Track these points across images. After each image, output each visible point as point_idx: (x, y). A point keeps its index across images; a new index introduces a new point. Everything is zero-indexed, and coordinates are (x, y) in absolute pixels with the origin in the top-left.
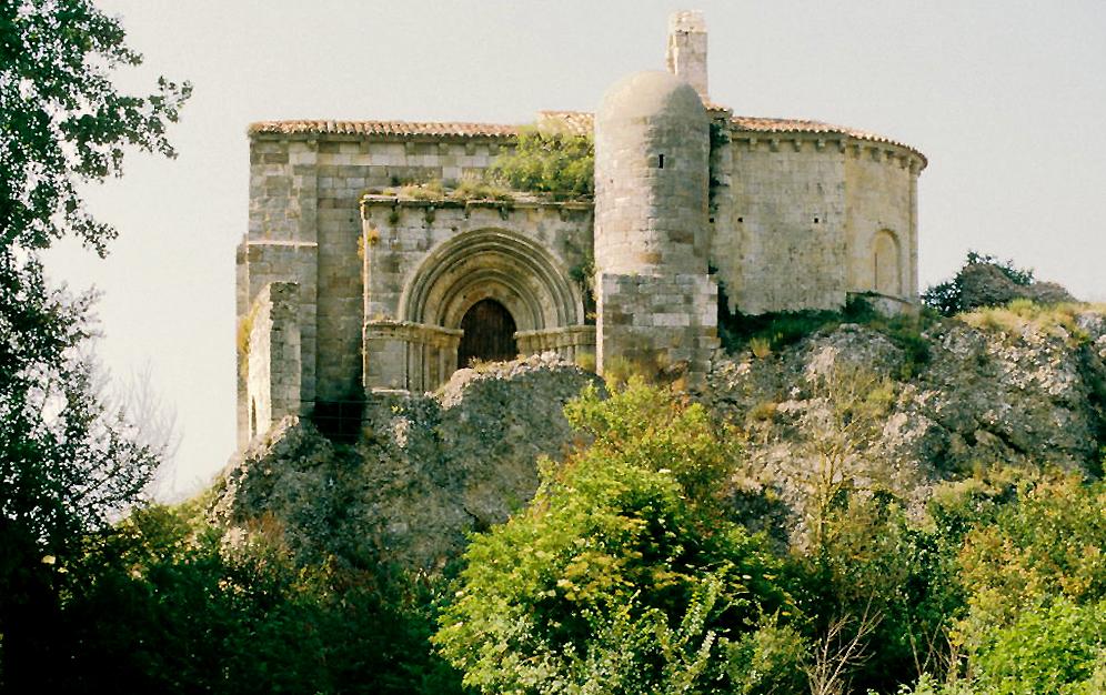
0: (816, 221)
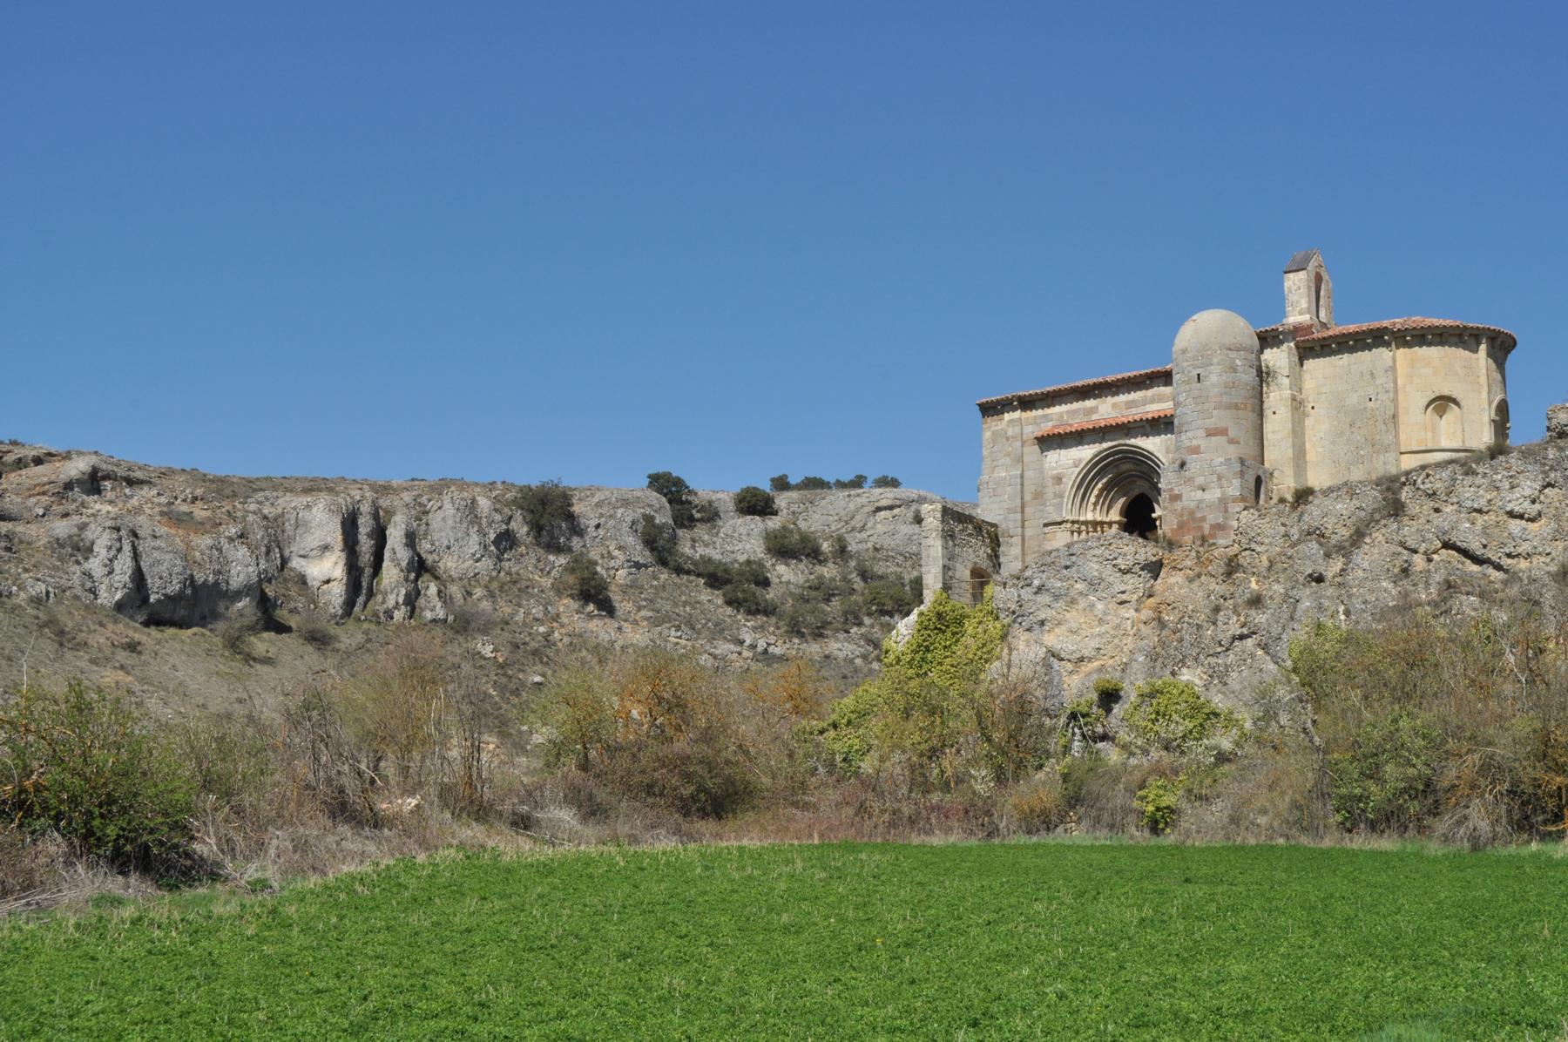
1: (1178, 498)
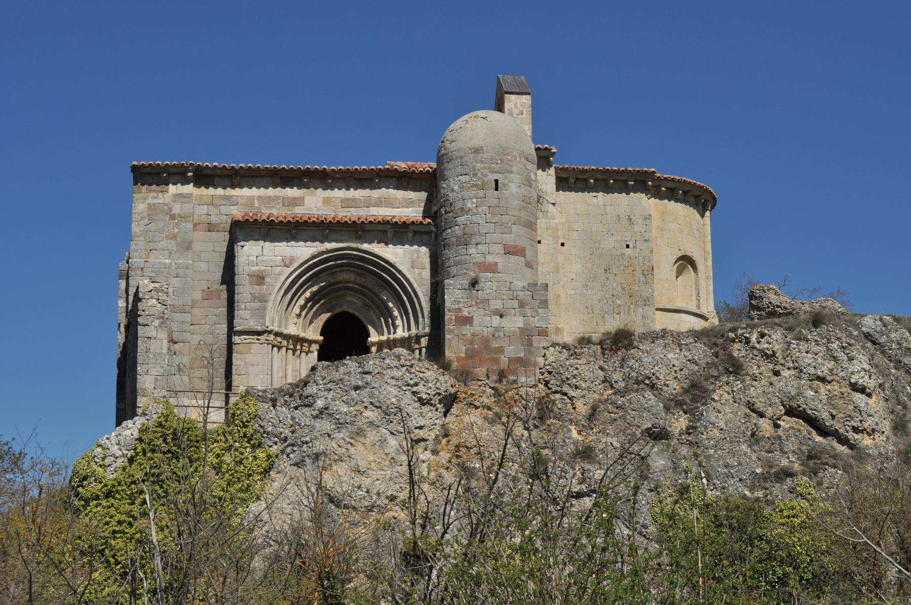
0: (628, 246)
1: (468, 320)
